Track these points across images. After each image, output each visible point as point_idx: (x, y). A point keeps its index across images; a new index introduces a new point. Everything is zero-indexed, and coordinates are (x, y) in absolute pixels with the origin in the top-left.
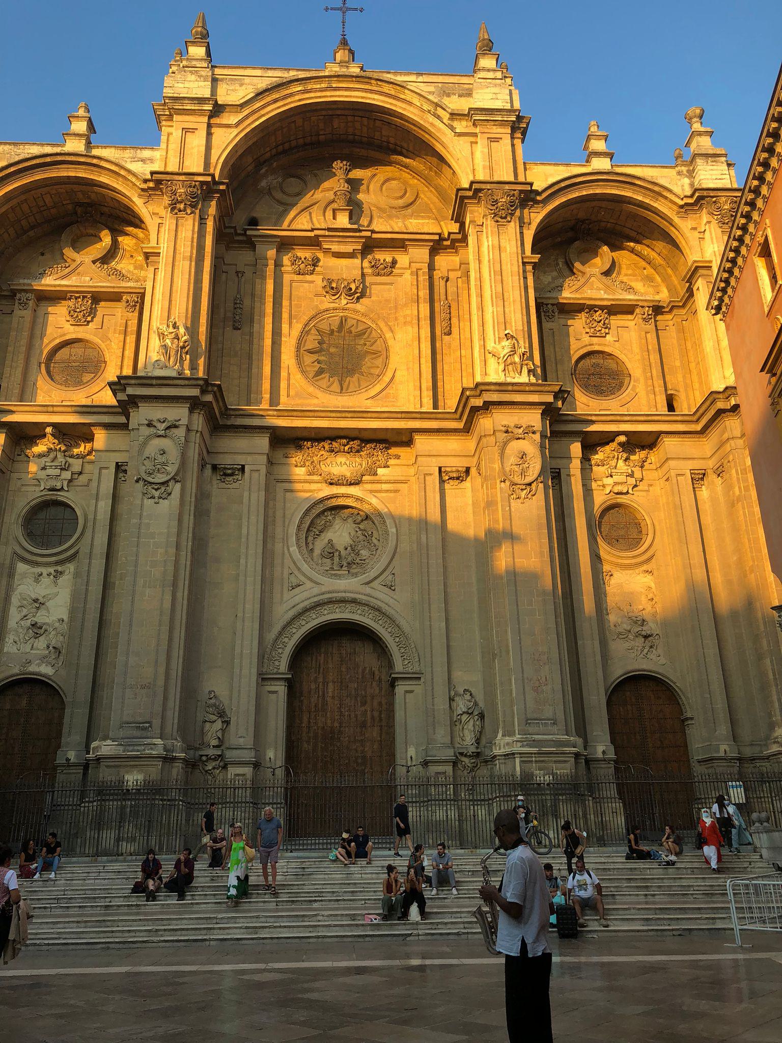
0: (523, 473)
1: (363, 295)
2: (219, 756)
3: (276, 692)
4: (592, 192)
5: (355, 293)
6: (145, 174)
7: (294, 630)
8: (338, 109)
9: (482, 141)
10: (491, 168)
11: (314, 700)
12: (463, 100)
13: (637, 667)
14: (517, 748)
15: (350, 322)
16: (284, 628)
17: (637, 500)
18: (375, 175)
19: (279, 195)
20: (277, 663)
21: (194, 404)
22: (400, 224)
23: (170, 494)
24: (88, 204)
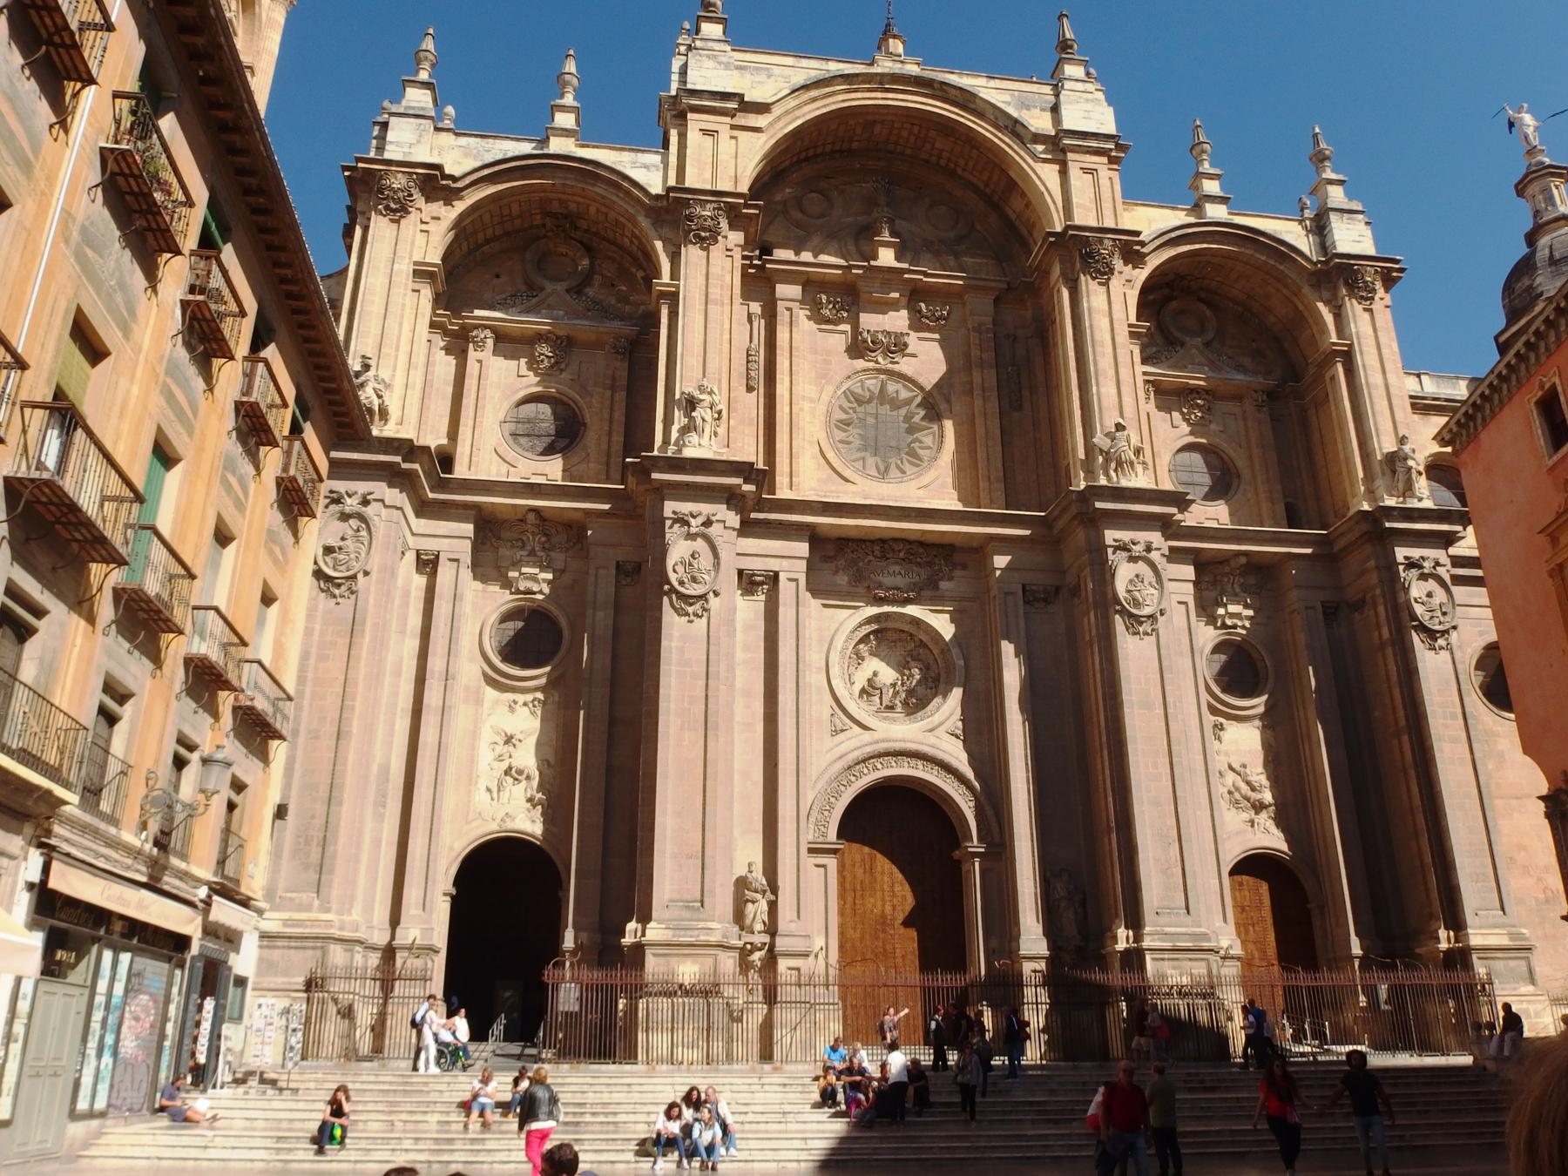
3: (824, 866)
19: (799, 216)
22: (952, 263)
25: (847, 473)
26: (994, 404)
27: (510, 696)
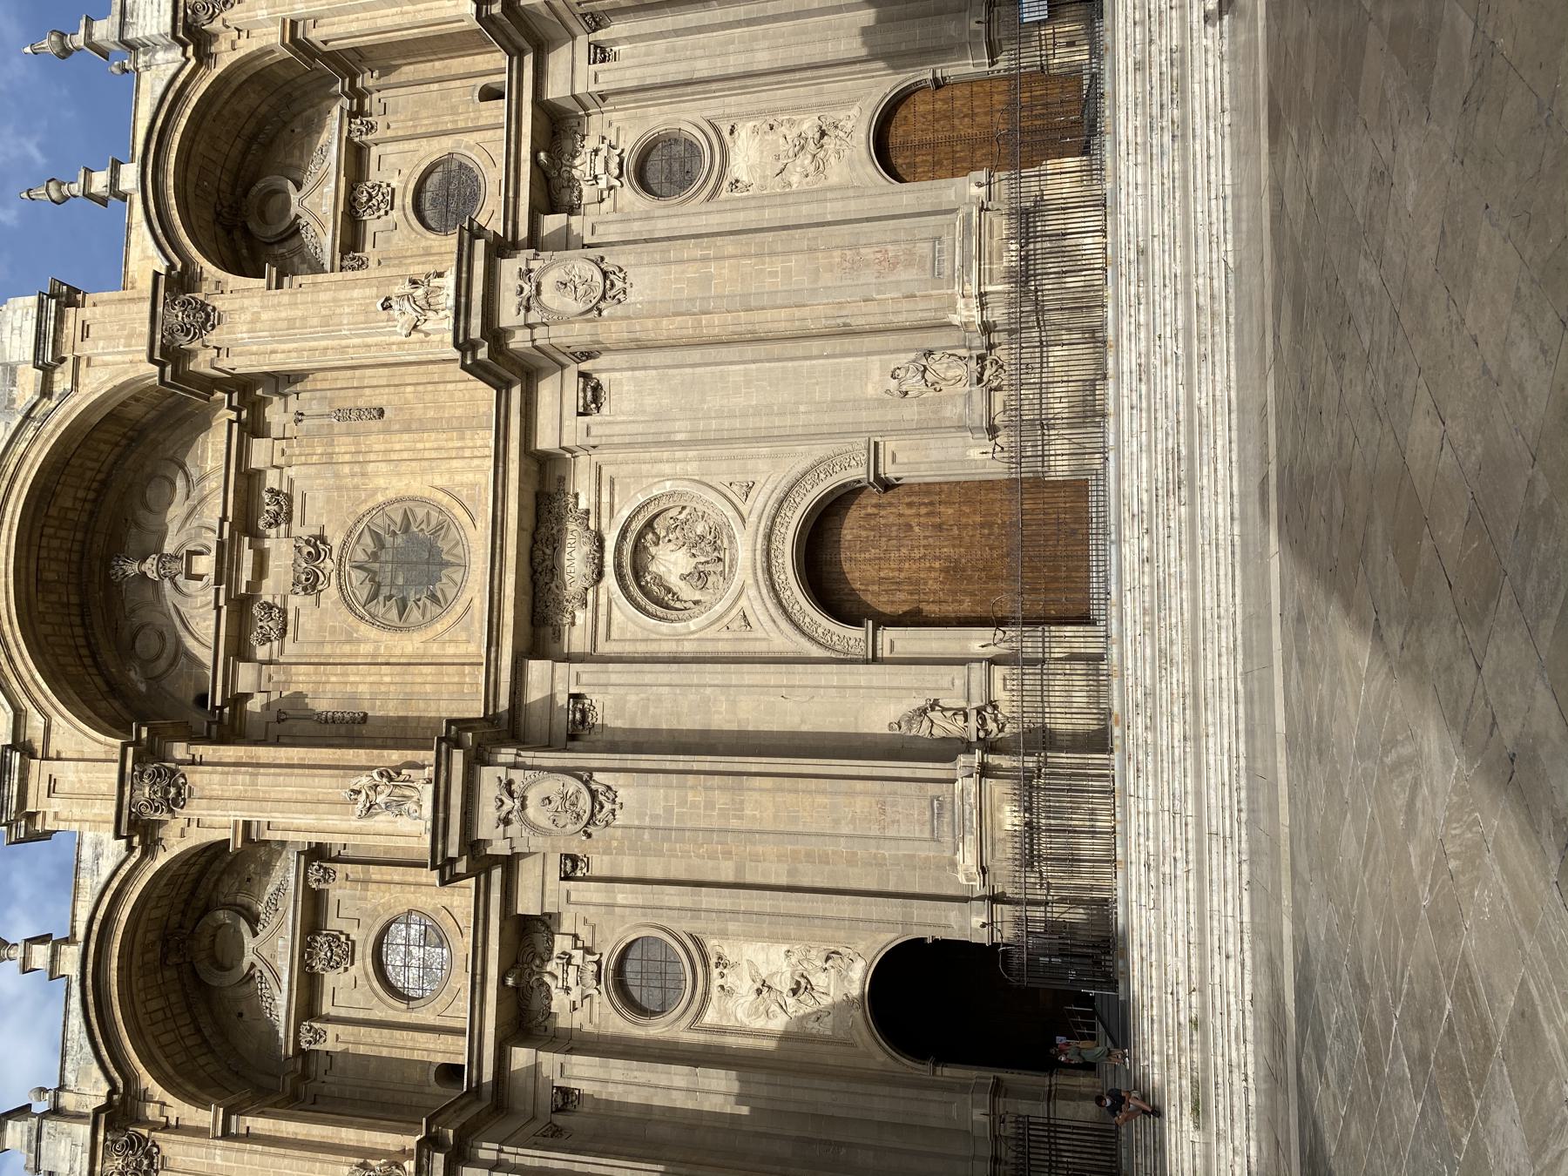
2: (979, 713)
4: (171, 192)
5: (315, 546)
6: (119, 853)
7: (807, 620)
8: (27, 568)
9: (85, 349)
10: (130, 336)
11: (902, 596)
12: (20, 380)
13: (863, 147)
14: (973, 289)
15: (360, 556)
16: (803, 633)
17: (629, 142)
18: (138, 525)
19: (163, 664)
20: (852, 643)
21: (478, 759)
23: (609, 788)
24: (163, 946)
25: (459, 609)
26: (376, 442)
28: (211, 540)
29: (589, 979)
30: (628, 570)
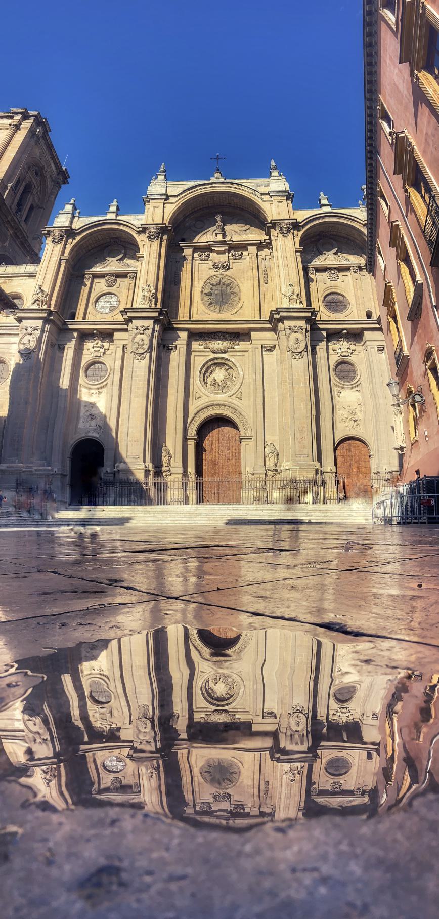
0: (298, 348)
1: (229, 268)
15: (223, 281)
27: (91, 391)
28: (228, 239)
29: (96, 354)
30: (216, 361)
